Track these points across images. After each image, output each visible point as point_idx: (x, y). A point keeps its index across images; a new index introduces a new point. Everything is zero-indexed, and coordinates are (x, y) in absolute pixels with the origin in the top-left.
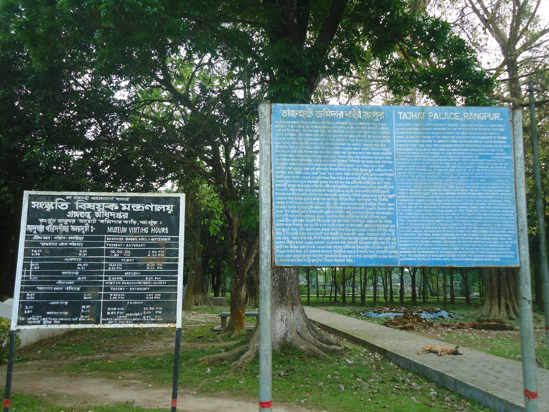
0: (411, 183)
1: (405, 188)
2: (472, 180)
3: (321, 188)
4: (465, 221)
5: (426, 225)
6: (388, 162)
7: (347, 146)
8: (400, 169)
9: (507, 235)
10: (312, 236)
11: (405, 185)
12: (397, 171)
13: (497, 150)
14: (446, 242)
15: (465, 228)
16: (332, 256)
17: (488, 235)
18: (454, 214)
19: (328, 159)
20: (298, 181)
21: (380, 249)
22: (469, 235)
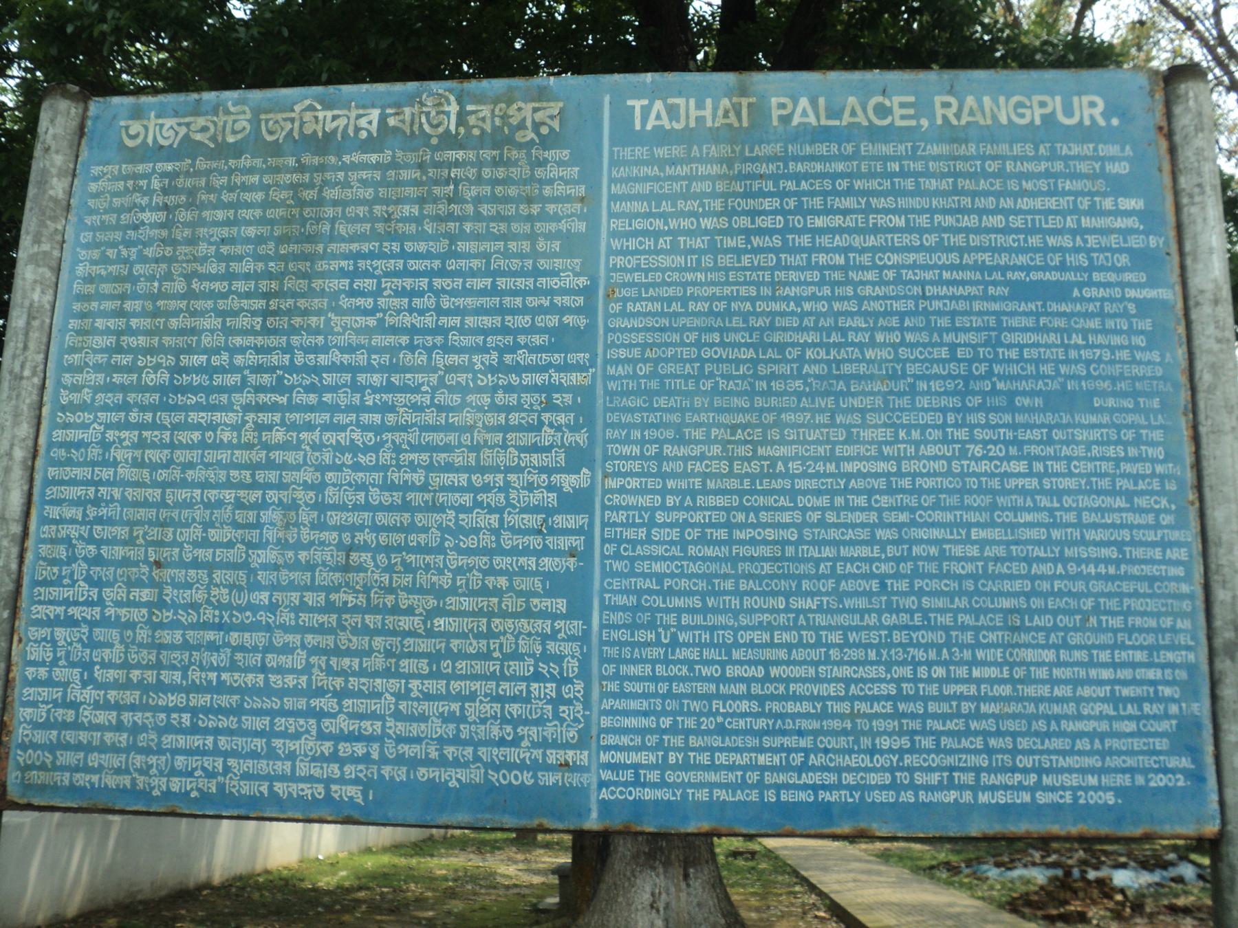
0: (675, 418)
1: (642, 442)
2: (977, 400)
3: (249, 446)
4: (941, 603)
5: (744, 621)
6: (569, 319)
7: (382, 256)
8: (623, 353)
9: (1152, 674)
10: (185, 669)
11: (644, 426)
12: (606, 362)
13: (1100, 259)
14: (844, 708)
15: (940, 637)
16: (263, 766)
17: (1057, 672)
18: (885, 568)
19: (289, 313)
20: (149, 416)
21: (502, 742)
22: (962, 672)
